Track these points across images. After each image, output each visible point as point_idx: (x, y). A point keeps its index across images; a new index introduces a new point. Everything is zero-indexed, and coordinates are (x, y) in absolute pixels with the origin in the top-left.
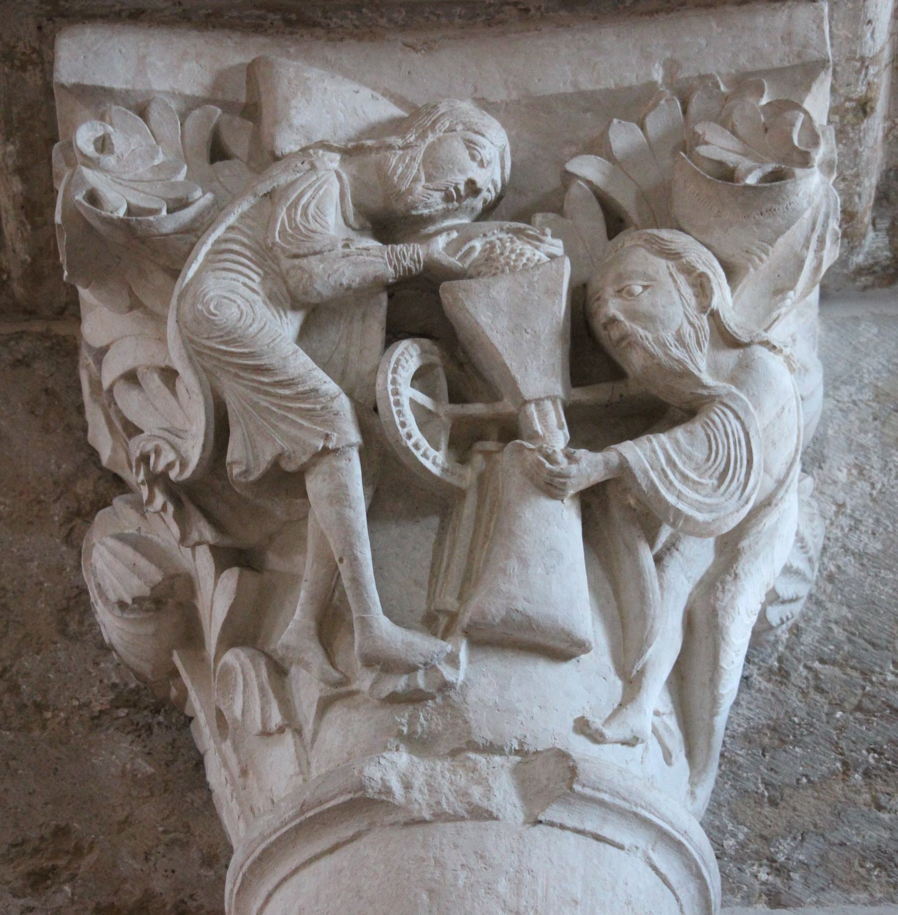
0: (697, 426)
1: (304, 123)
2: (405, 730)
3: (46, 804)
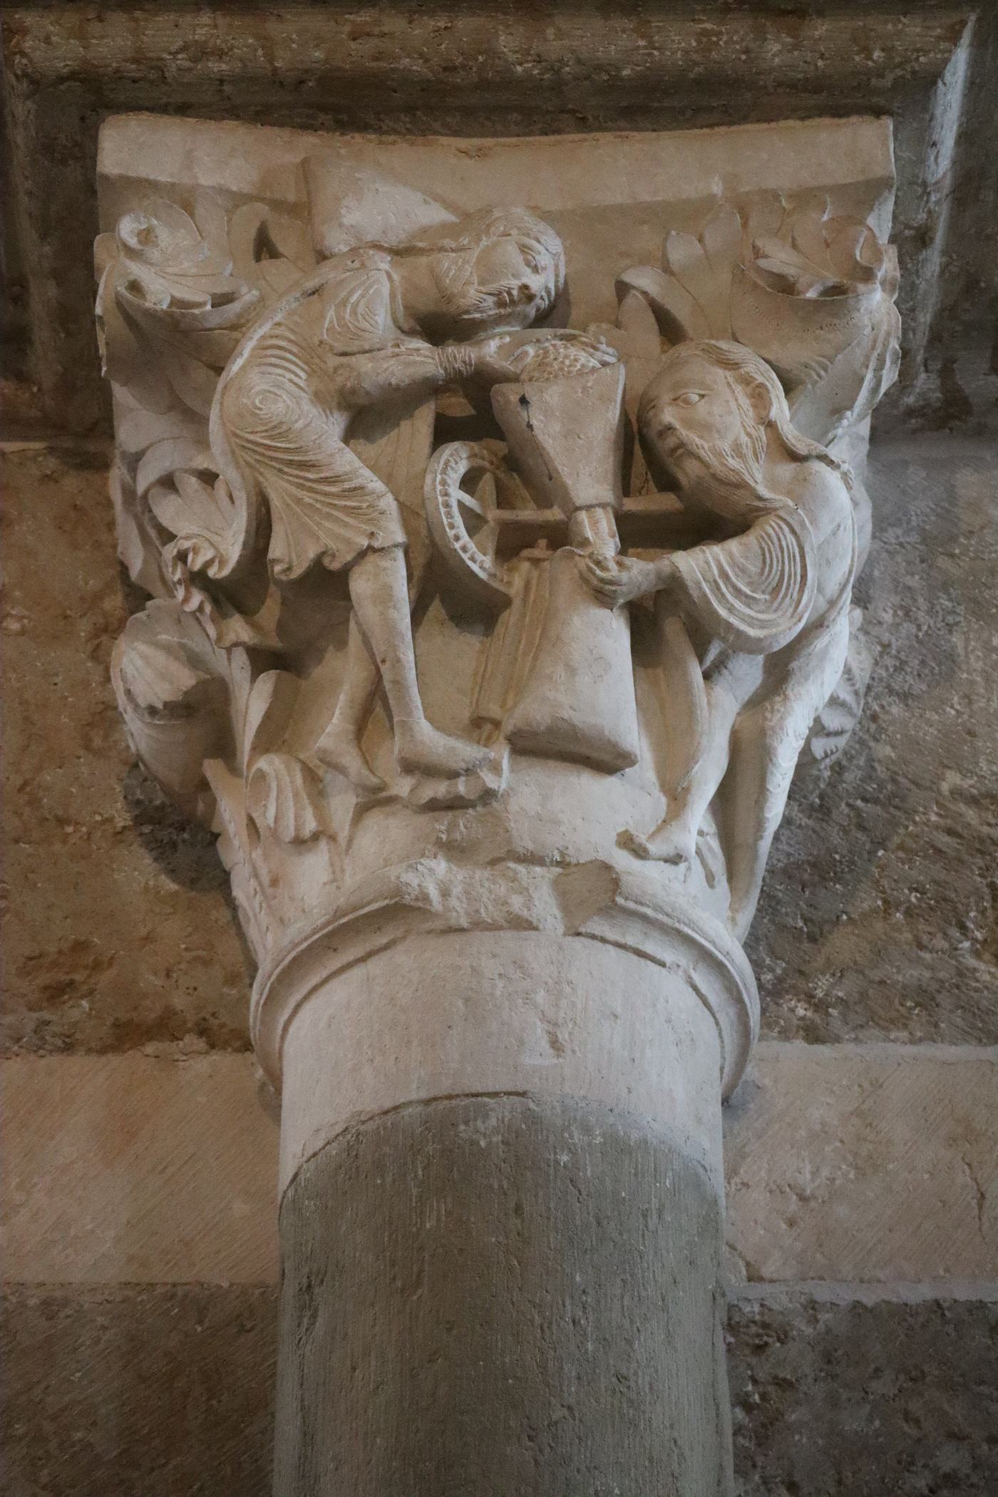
0: (751, 538)
1: (353, 223)
2: (444, 837)
3: (66, 918)
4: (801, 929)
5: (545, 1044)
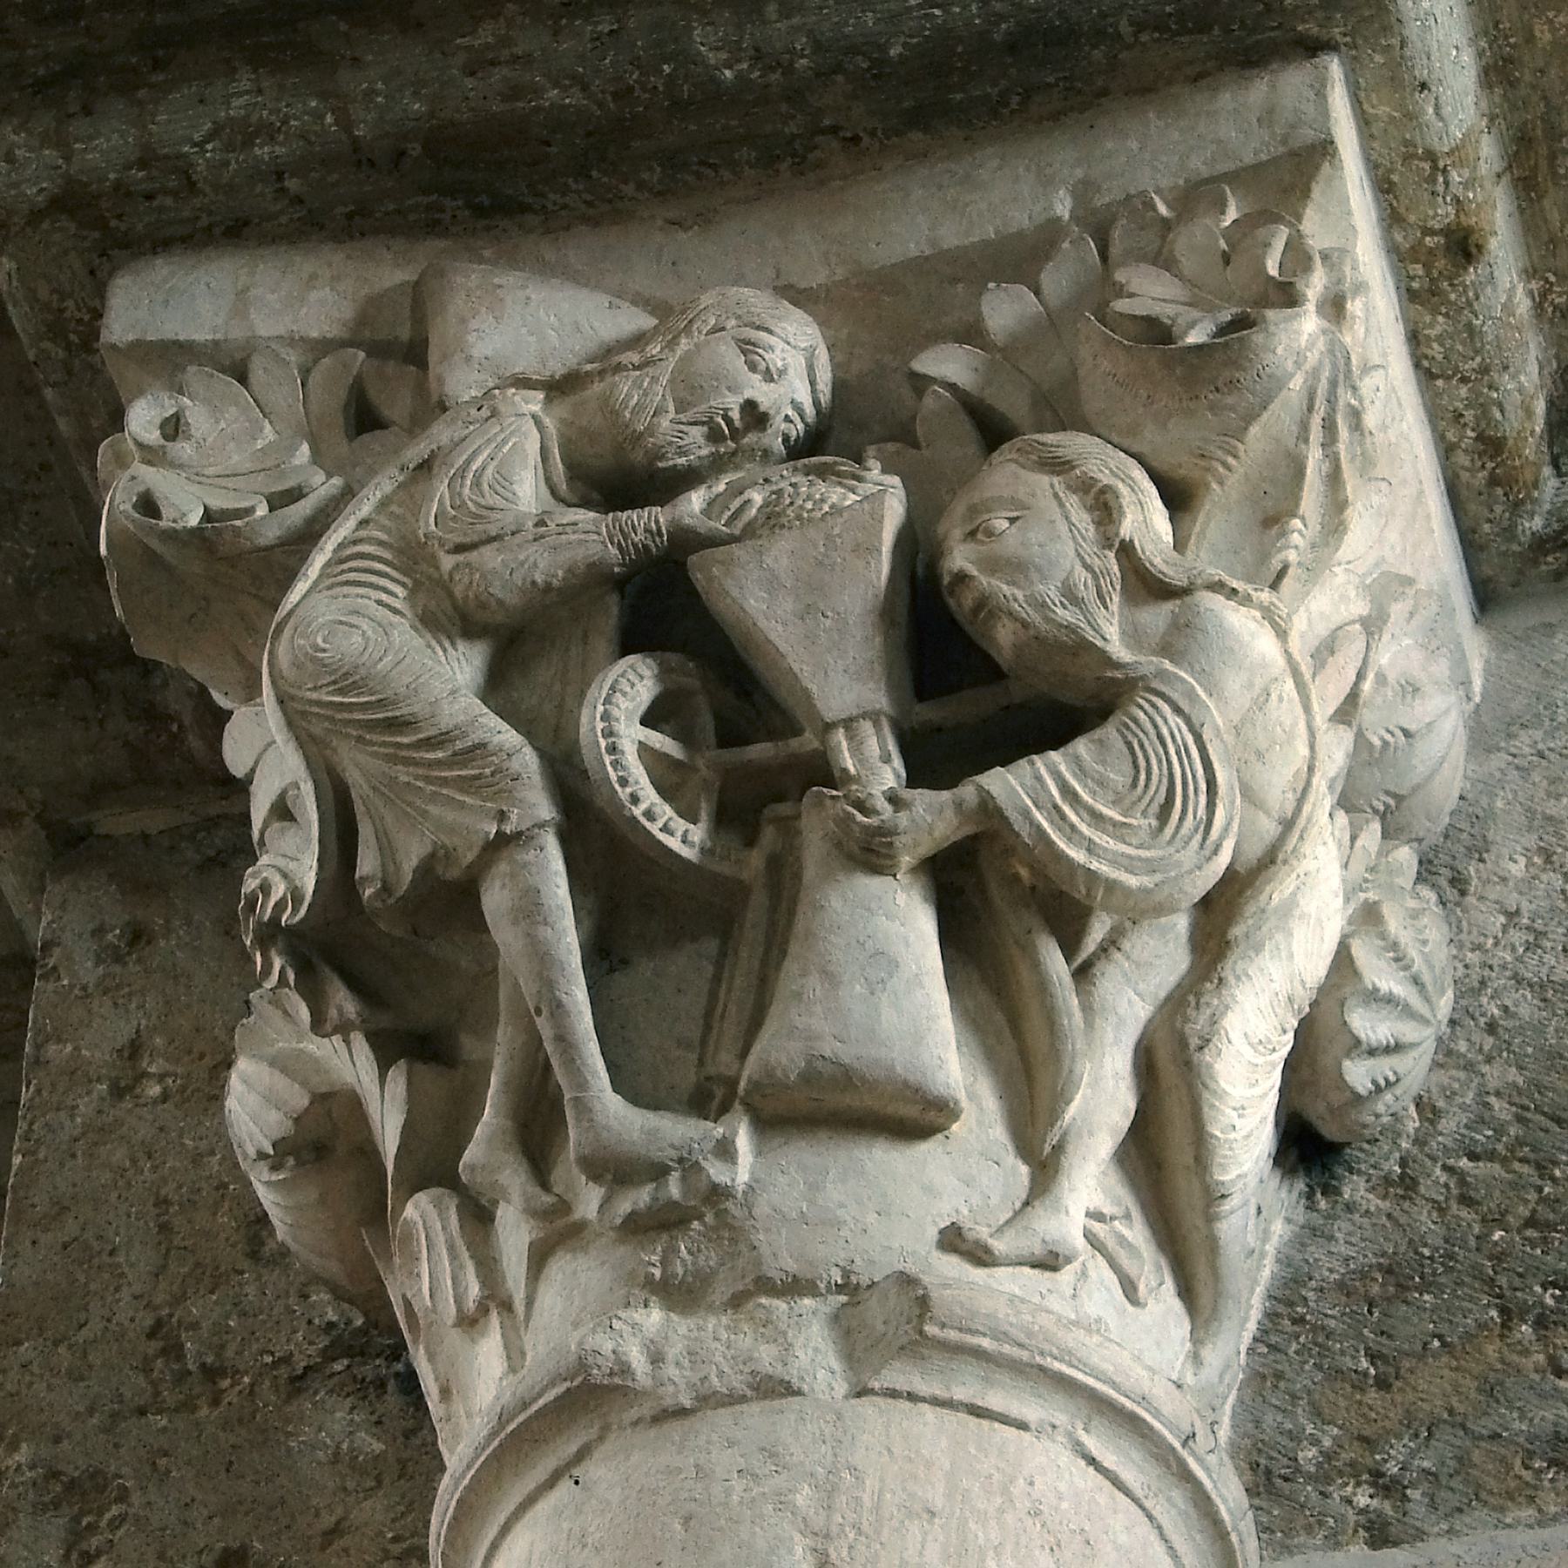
0: (1109, 731)
1: (489, 353)
2: (657, 1273)
4: (1366, 1374)
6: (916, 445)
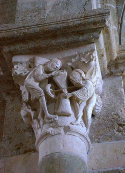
0: (81, 89)
5: (62, 147)
6: (67, 69)
